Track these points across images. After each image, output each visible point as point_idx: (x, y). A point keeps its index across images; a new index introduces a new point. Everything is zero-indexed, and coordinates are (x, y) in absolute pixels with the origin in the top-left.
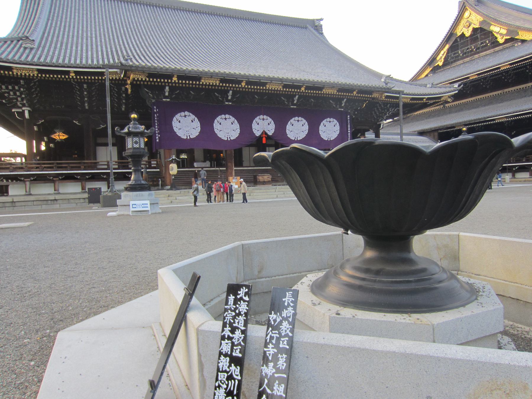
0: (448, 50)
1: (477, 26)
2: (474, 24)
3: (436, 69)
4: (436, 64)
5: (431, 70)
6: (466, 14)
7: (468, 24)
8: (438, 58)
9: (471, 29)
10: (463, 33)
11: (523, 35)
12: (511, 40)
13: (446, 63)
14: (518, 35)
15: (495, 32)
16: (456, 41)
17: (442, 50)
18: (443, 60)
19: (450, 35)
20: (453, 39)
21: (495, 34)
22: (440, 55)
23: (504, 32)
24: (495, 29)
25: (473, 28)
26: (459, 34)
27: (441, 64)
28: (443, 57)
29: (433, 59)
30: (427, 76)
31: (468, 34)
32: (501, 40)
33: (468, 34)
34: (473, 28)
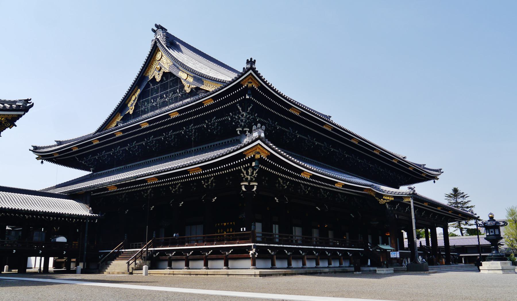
0: (140, 96)
1: (167, 71)
2: (165, 68)
3: (126, 118)
4: (127, 112)
6: (159, 56)
7: (158, 67)
8: (129, 105)
10: (154, 76)
15: (183, 79)
16: (148, 86)
17: (134, 95)
18: (133, 107)
19: (141, 79)
20: (145, 84)
21: (183, 81)
22: (132, 102)
24: (182, 75)
26: (150, 78)
27: (131, 113)
28: (134, 104)
29: (122, 107)
31: (158, 79)
33: (158, 79)
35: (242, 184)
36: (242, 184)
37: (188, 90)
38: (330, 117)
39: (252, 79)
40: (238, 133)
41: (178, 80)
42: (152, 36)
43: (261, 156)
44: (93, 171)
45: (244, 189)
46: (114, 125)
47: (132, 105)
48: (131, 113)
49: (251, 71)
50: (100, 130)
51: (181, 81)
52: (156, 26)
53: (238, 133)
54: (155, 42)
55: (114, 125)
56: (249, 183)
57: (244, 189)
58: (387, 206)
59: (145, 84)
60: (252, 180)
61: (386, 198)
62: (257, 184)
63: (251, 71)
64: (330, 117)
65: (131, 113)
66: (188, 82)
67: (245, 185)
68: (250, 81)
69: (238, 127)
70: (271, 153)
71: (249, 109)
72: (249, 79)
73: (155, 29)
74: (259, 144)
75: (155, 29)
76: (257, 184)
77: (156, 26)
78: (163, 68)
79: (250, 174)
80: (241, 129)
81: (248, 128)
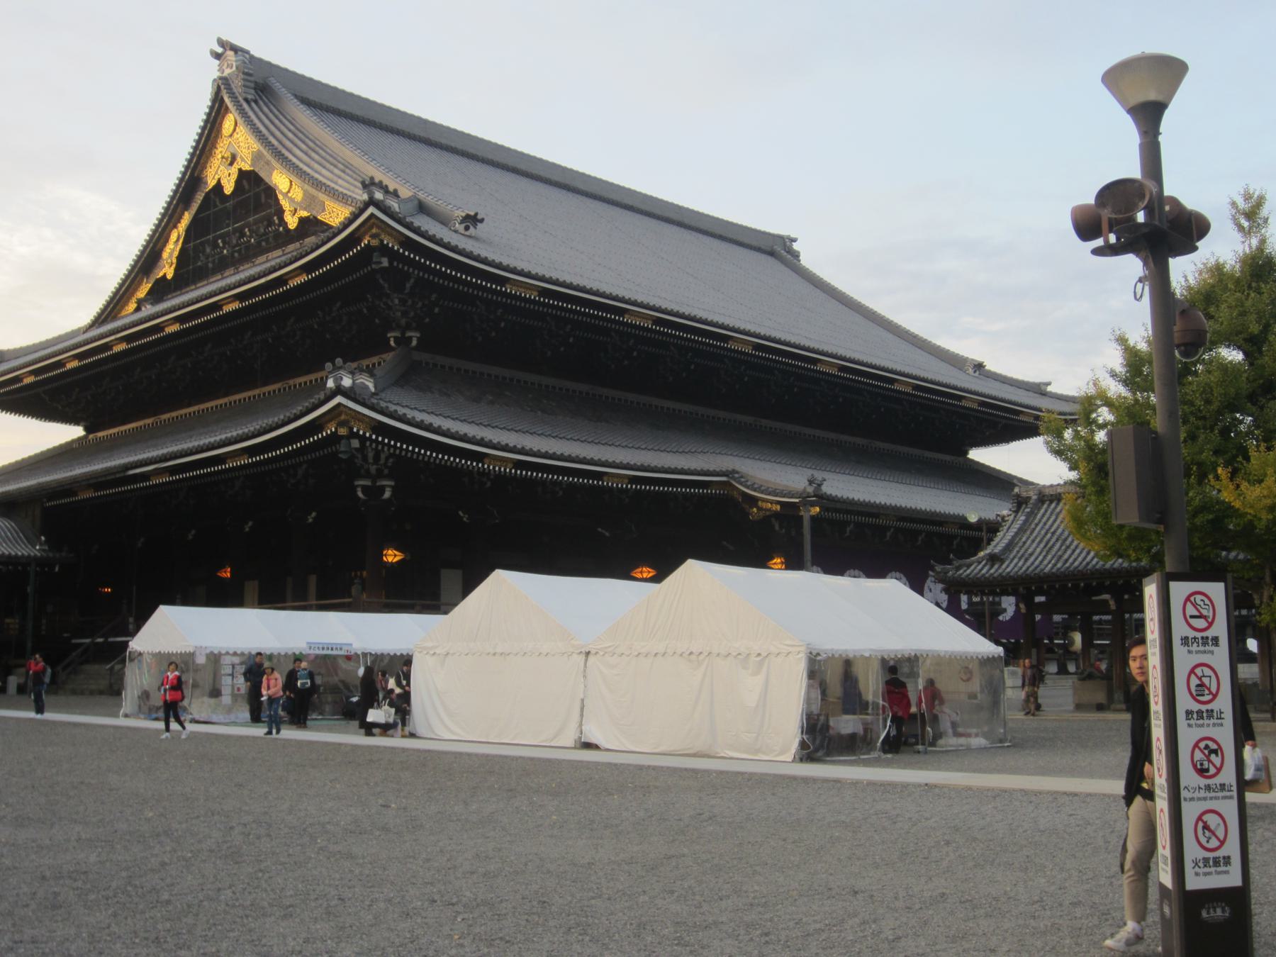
1: (247, 167)
3: (161, 290)
4: (161, 274)
5: (148, 294)
7: (228, 155)
8: (165, 255)
9: (234, 171)
11: (335, 214)
12: (310, 225)
13: (189, 271)
14: (324, 210)
15: (281, 192)
17: (175, 227)
18: (175, 261)
20: (199, 198)
21: (280, 197)
22: (170, 246)
23: (297, 194)
24: (280, 180)
25: (240, 170)
26: (211, 183)
28: (176, 253)
30: (138, 309)
31: (229, 188)
32: (292, 222)
34: (240, 170)
35: (356, 483)
36: (356, 483)
37: (292, 222)
38: (794, 240)
39: (378, 227)
40: (392, 343)
41: (271, 192)
42: (212, 70)
43: (351, 429)
44: (86, 429)
45: (360, 494)
46: (132, 306)
47: (171, 255)
48: (169, 277)
49: (371, 210)
50: (99, 320)
51: (277, 200)
52: (221, 43)
53: (392, 343)
54: (219, 87)
55: (132, 306)
56: (374, 482)
57: (360, 494)
58: (777, 528)
59: (199, 198)
60: (379, 475)
61: (764, 505)
62: (392, 483)
63: (371, 210)
64: (794, 240)
65: (169, 277)
66: (292, 200)
67: (364, 488)
68: (374, 231)
69: (393, 330)
70: (380, 422)
71: (408, 285)
72: (372, 227)
73: (220, 50)
74: (339, 405)
75: (220, 50)
76: (392, 483)
77: (221, 43)
78: (239, 159)
79: (371, 460)
80: (397, 334)
81: (416, 330)
